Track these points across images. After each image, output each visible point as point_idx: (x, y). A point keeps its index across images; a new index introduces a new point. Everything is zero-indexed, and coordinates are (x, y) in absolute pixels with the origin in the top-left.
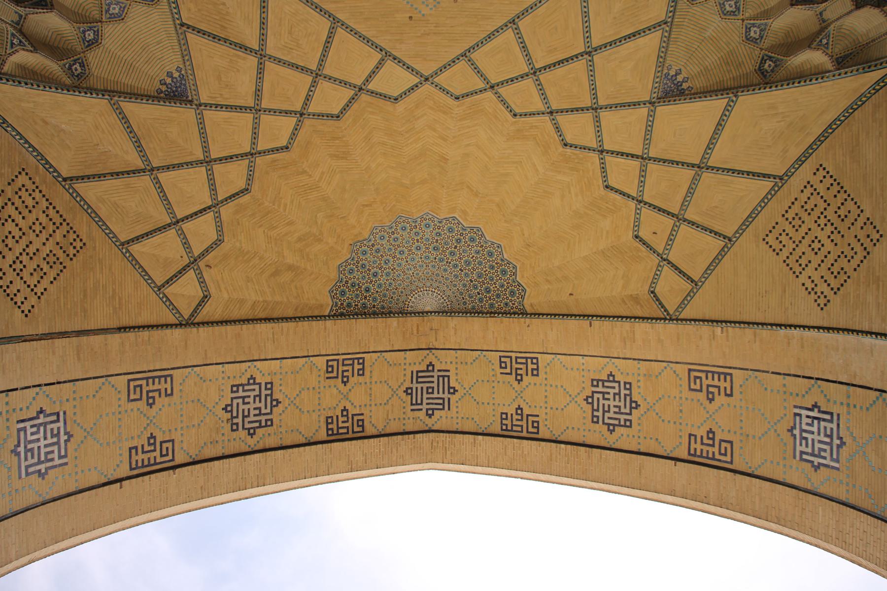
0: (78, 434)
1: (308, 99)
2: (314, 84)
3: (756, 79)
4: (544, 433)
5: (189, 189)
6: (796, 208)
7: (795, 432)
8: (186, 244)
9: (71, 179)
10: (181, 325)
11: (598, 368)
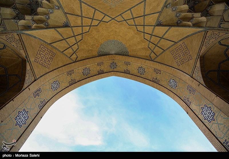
0: (61, 83)
1: (91, 23)
2: (92, 21)
3: (176, 24)
4: (130, 73)
5: (72, 41)
6: (178, 48)
7: (170, 82)
8: (73, 50)
9: (50, 44)
10: (74, 62)
11: (139, 65)
